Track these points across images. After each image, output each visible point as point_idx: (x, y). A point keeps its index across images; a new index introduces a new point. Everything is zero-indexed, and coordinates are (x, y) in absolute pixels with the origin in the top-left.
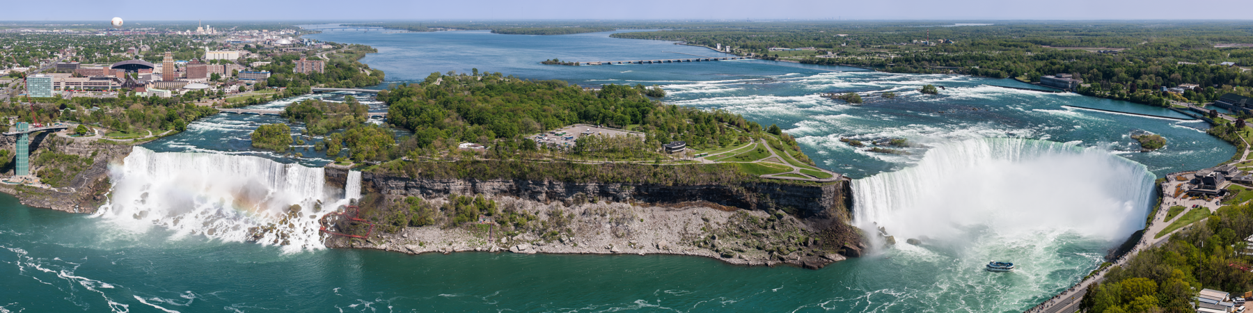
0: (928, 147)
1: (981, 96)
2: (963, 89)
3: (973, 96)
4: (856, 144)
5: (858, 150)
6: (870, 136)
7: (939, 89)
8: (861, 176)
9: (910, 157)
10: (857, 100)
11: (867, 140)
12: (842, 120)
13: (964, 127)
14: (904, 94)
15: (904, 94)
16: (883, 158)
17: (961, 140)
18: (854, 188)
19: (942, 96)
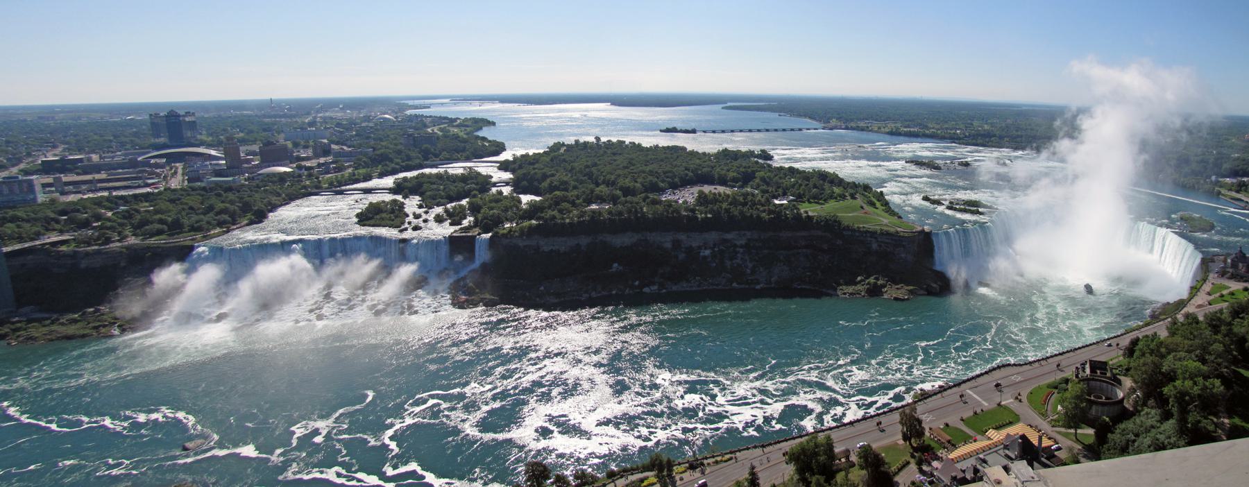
4: (938, 202)
5: (940, 209)
6: (947, 197)
9: (981, 216)
10: (938, 168)
11: (946, 200)
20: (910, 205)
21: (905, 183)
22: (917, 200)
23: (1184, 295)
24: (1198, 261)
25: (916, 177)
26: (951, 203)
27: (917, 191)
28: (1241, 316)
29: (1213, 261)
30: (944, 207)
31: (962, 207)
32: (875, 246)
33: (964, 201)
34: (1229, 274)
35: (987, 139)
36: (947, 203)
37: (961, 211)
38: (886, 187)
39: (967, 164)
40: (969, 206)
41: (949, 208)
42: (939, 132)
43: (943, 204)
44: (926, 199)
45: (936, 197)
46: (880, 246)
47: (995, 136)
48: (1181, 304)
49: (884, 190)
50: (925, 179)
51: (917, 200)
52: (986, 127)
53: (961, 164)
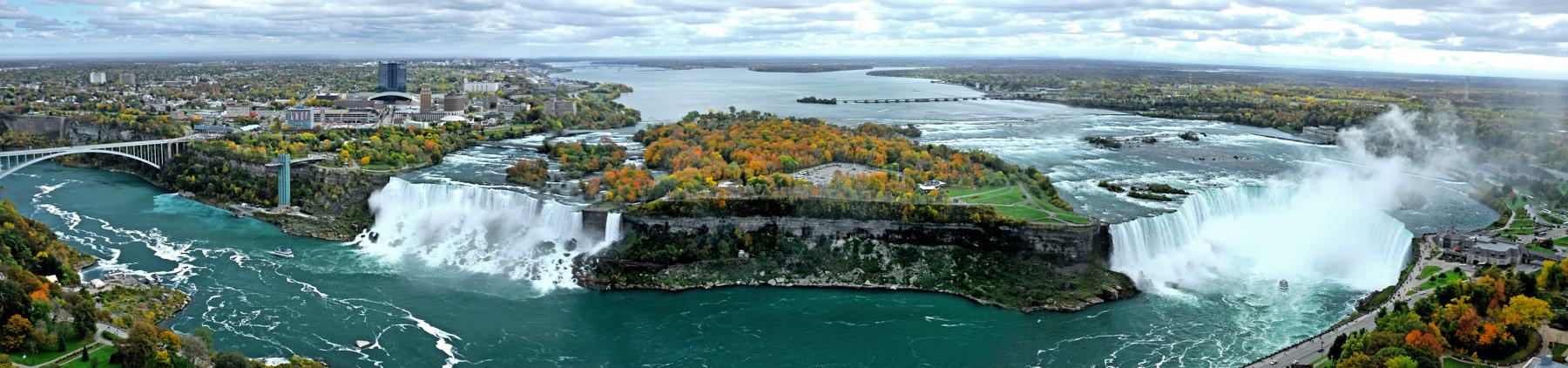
0: (1188, 194)
1: (1239, 144)
2: (1225, 136)
3: (1235, 144)
4: (1118, 189)
5: (1120, 196)
6: (1129, 181)
7: (1200, 136)
8: (1119, 221)
9: (1169, 203)
10: (1117, 146)
11: (1126, 185)
12: (1103, 165)
13: (1225, 175)
14: (1164, 139)
15: (1164, 139)
16: (1142, 203)
17: (1221, 188)
18: (1112, 230)
19: (1204, 143)
20: (1083, 194)
21: (1077, 166)
22: (1092, 186)
23: (1395, 282)
24: (1409, 242)
25: (1092, 157)
26: (1133, 188)
27: (1091, 175)
28: (1452, 300)
29: (1424, 240)
30: (1125, 194)
31: (1146, 193)
32: (1039, 246)
33: (1148, 185)
34: (1441, 254)
35: (1178, 110)
36: (1128, 189)
37: (1144, 197)
38: (1053, 171)
39: (1153, 141)
40: (1154, 191)
41: (1132, 195)
42: (1120, 101)
43: (1124, 190)
44: (1103, 185)
45: (1116, 182)
46: (1045, 246)
47: (1186, 105)
48: (1392, 290)
49: (1050, 175)
50: (1103, 160)
51: (1092, 186)
52: (1176, 95)
53: (1145, 141)
